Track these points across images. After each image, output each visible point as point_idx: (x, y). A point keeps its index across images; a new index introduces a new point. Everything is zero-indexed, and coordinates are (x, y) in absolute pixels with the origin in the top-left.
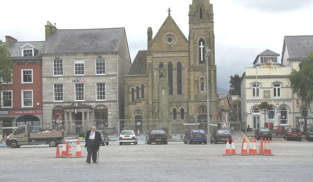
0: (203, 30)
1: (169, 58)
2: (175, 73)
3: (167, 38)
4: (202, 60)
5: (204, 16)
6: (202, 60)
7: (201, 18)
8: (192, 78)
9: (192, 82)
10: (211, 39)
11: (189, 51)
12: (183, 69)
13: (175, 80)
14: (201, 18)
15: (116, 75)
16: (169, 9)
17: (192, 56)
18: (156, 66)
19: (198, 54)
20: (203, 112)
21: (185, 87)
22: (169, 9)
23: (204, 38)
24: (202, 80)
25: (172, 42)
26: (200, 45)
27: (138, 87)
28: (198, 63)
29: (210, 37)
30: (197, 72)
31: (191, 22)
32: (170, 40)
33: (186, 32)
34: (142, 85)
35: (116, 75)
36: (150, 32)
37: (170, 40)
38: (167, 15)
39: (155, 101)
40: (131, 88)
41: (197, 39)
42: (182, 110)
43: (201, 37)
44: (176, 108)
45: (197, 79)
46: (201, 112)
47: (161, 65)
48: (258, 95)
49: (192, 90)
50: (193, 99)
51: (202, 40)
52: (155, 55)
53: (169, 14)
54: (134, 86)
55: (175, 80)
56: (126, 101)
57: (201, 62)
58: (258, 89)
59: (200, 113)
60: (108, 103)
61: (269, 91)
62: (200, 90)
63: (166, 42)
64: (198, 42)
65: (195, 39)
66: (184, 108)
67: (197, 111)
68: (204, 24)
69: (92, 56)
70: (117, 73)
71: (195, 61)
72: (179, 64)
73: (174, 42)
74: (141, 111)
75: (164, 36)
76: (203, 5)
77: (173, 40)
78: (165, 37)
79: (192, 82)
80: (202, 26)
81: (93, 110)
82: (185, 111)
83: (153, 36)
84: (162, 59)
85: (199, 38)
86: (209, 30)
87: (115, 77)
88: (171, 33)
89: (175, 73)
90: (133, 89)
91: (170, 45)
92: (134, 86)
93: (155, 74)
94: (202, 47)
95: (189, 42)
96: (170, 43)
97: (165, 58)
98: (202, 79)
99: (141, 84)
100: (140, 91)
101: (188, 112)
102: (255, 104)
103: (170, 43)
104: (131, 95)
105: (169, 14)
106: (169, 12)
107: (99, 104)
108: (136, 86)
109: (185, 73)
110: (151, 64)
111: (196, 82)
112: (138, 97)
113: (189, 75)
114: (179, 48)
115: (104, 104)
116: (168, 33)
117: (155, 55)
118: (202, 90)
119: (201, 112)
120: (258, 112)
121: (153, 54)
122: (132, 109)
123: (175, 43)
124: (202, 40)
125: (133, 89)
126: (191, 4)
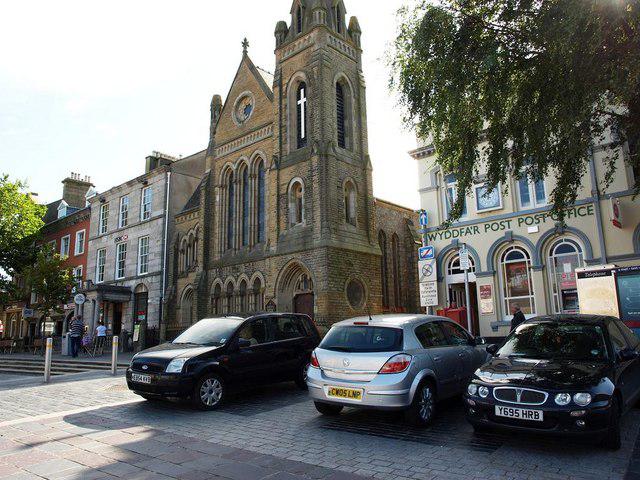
4: (303, 136)
6: (303, 136)
16: (245, 40)
22: (245, 40)
26: (299, 98)
41: (287, 84)
46: (302, 285)
53: (245, 52)
60: (149, 279)
81: (133, 295)
88: (246, 92)
105: (245, 52)
107: (139, 281)
115: (144, 281)
119: (302, 285)
124: (302, 85)
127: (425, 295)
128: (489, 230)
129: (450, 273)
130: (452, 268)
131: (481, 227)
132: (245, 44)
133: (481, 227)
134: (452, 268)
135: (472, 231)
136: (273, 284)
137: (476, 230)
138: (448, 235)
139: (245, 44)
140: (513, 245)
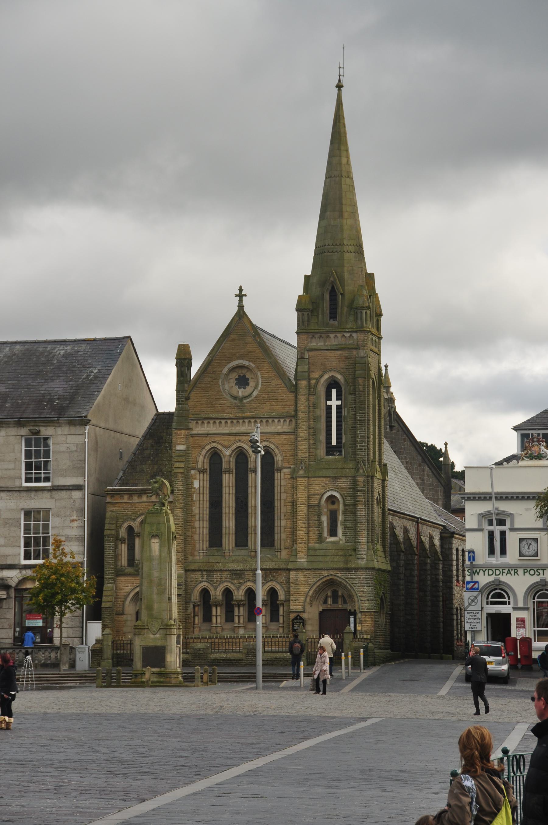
0: (338, 353)
1: (238, 438)
2: (255, 481)
3: (234, 375)
4: (334, 443)
5: (343, 310)
6: (334, 443)
7: (333, 316)
8: (302, 498)
9: (302, 511)
10: (361, 381)
11: (295, 416)
12: (279, 470)
13: (255, 501)
14: (333, 316)
15: (79, 488)
16: (241, 290)
17: (303, 432)
18: (202, 460)
20: (335, 601)
21: (281, 523)
22: (241, 290)
23: (339, 377)
24: (333, 503)
25: (249, 389)
26: (329, 397)
28: (322, 451)
30: (318, 481)
31: (303, 330)
33: (289, 360)
35: (79, 488)
37: (243, 382)
38: (236, 309)
39: (192, 567)
40: (126, 525)
41: (318, 380)
43: (332, 374)
45: (314, 502)
46: (330, 601)
47: (215, 457)
48: (503, 552)
49: (301, 533)
50: (302, 560)
51: (333, 384)
52: (199, 429)
53: (241, 306)
54: (134, 520)
55: (255, 501)
56: (109, 564)
57: (330, 450)
58: (503, 534)
59: (325, 602)
61: (536, 540)
62: (325, 534)
65: (313, 382)
66: (278, 587)
67: (314, 597)
68: (339, 335)
69: (13, 431)
70: (85, 481)
71: (313, 446)
73: (253, 390)
75: (225, 371)
76: (342, 280)
77: (252, 383)
78: (227, 375)
79: (302, 511)
80: (334, 340)
81: (12, 593)
82: (282, 596)
84: (217, 439)
85: (326, 377)
86: (354, 352)
87: (76, 494)
88: (246, 363)
89: (255, 481)
90: (130, 529)
91: (241, 399)
93: (196, 484)
94: (334, 403)
95: (295, 389)
96: (241, 393)
97: (226, 438)
98: (332, 500)
101: (288, 600)
102: (492, 578)
103: (241, 393)
104: (124, 548)
105: (241, 306)
106: (241, 301)
107: (29, 573)
109: (281, 479)
110: (185, 455)
111: (314, 509)
113: (294, 488)
114: (265, 409)
116: (236, 363)
117: (199, 429)
118: (333, 532)
119: (330, 601)
120: (504, 603)
121: (192, 424)
122: (127, 589)
123: (255, 393)
124: (333, 384)
125: (130, 529)
126: (309, 273)
127: (470, 621)
128: (527, 574)
129: (487, 604)
130: (490, 599)
131: (521, 571)
132: (241, 295)
133: (521, 571)
134: (490, 599)
135: (512, 572)
136: (303, 598)
137: (516, 573)
138: (491, 572)
139: (241, 295)
140: (544, 588)
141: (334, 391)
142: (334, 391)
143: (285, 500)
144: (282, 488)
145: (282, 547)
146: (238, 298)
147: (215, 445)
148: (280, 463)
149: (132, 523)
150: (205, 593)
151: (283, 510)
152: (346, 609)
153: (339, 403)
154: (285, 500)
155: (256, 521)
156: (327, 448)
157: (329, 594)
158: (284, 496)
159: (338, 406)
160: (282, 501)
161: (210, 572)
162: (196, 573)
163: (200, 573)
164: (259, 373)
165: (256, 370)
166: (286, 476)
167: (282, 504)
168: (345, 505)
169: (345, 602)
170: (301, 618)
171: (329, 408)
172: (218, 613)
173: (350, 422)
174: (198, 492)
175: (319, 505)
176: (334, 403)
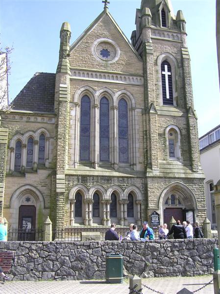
1: (106, 86)
4: (168, 97)
6: (168, 97)
9: (155, 136)
12: (133, 109)
17: (151, 86)
19: (160, 84)
20: (173, 203)
23: (171, 57)
26: (163, 70)
27: (31, 139)
28: (161, 100)
29: (184, 56)
32: (105, 53)
34: (42, 135)
36: (64, 35)
42: (131, 195)
44: (119, 190)
51: (165, 62)
54: (23, 134)
63: (97, 56)
64: (160, 62)
66: (137, 191)
72: (123, 100)
74: (37, 198)
82: (139, 196)
83: (72, 41)
84: (90, 84)
88: (110, 41)
92: (23, 134)
99: (39, 131)
100: (36, 148)
105: (105, 8)
108: (27, 135)
112: (29, 162)
141: (166, 67)
142: (166, 67)
143: (138, 130)
144: (136, 121)
145: (137, 162)
146: (104, 4)
147: (88, 88)
148: (134, 104)
149: (21, 137)
150: (79, 195)
151: (137, 136)
152: (181, 208)
153: (170, 73)
154: (138, 130)
155: (116, 143)
156: (163, 100)
157: (170, 197)
158: (137, 127)
159: (168, 75)
160: (136, 130)
161: (84, 179)
162: (74, 177)
163: (76, 177)
164: (118, 49)
165: (116, 46)
166: (138, 114)
167: (137, 132)
168: (181, 135)
169: (180, 203)
170: (157, 214)
171: (163, 76)
172: (89, 209)
173: (180, 84)
174: (74, 118)
175: (164, 134)
176: (166, 73)
